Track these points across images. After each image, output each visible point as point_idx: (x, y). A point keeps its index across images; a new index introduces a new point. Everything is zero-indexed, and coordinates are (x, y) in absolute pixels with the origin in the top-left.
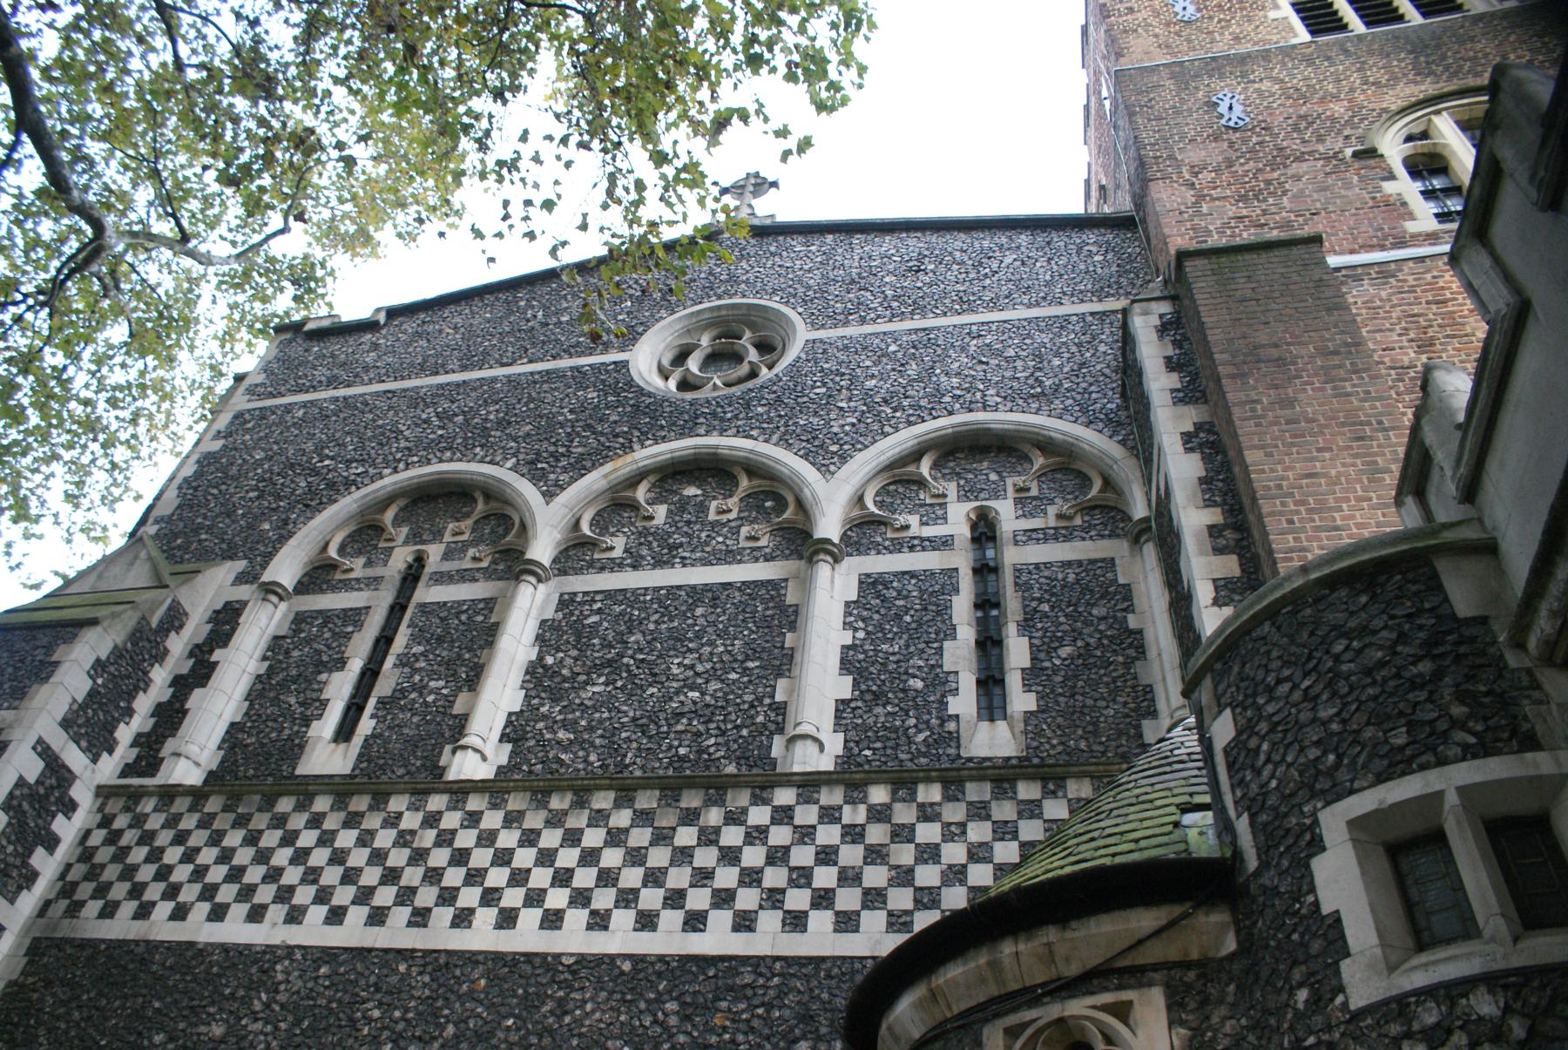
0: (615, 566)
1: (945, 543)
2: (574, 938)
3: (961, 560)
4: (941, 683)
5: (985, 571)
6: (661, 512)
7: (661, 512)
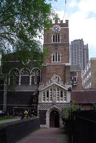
0: (23, 74)
1: (34, 74)
2: (24, 91)
3: (35, 75)
4: (34, 81)
5: (36, 75)
6: (24, 71)
7: (24, 71)
